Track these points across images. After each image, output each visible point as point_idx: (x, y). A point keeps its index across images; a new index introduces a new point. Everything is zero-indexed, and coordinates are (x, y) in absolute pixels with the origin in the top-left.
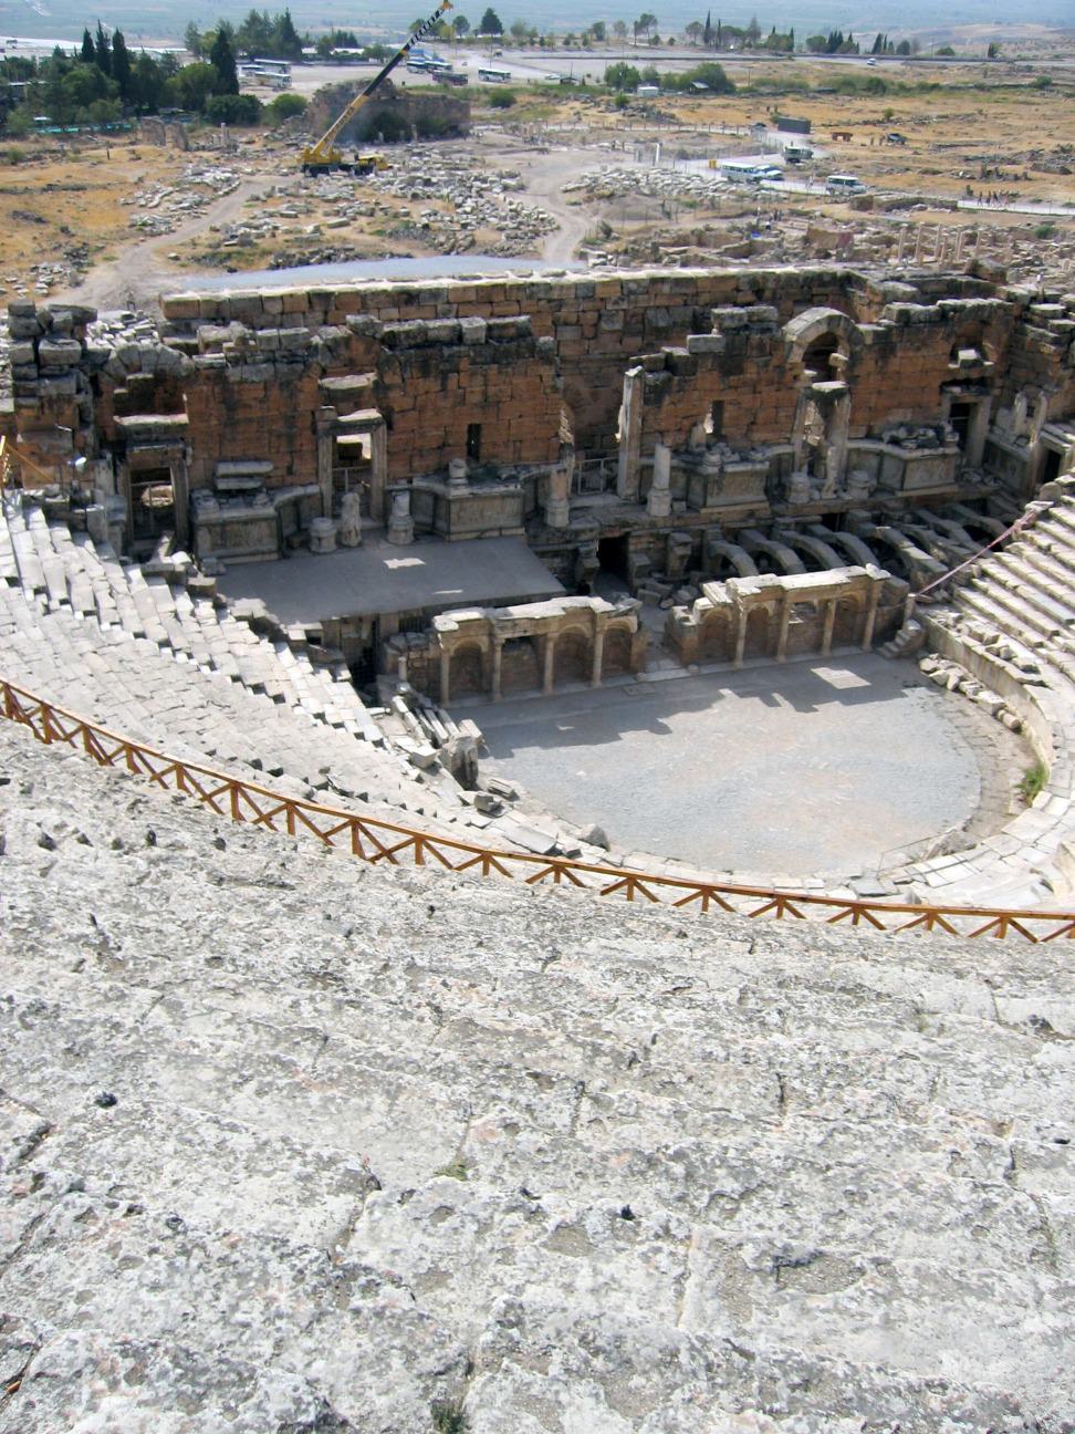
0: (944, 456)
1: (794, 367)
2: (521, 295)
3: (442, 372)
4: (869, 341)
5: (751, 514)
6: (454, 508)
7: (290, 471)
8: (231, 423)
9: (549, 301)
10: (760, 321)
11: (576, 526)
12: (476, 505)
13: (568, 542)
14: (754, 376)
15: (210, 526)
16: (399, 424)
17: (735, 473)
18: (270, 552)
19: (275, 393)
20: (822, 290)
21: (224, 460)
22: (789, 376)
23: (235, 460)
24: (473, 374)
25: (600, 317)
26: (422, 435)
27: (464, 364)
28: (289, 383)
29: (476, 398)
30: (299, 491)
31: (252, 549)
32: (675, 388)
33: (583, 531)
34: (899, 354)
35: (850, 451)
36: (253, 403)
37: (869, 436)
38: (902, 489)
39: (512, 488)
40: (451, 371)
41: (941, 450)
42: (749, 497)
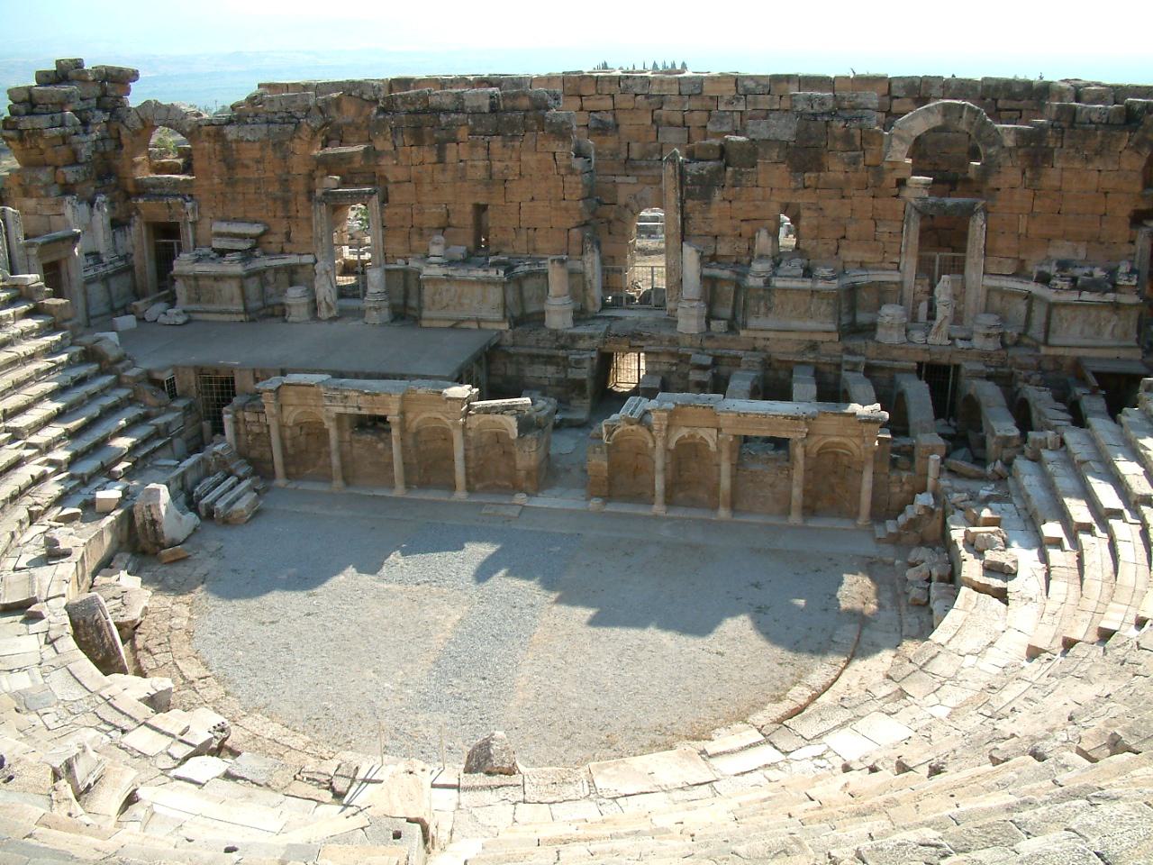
0: (1116, 307)
1: (895, 165)
2: (614, 88)
3: (438, 141)
4: (1009, 142)
5: (813, 346)
6: (428, 290)
7: (288, 234)
8: (231, 183)
9: (648, 96)
10: (854, 108)
11: (580, 330)
12: (454, 288)
13: (563, 347)
14: (842, 177)
15: (185, 277)
16: (395, 197)
17: (785, 290)
18: (238, 313)
19: (269, 153)
20: (1014, 104)
21: (225, 220)
22: (890, 180)
23: (236, 220)
24: (473, 146)
25: (710, 116)
26: (421, 212)
27: (463, 133)
28: (281, 143)
29: (480, 174)
30: (293, 260)
31: (224, 307)
32: (729, 182)
33: (581, 337)
34: (1058, 165)
35: (990, 290)
36: (251, 163)
37: (1020, 273)
38: (1046, 343)
39: (492, 273)
40: (449, 141)
41: (1110, 297)
42: (811, 325)
